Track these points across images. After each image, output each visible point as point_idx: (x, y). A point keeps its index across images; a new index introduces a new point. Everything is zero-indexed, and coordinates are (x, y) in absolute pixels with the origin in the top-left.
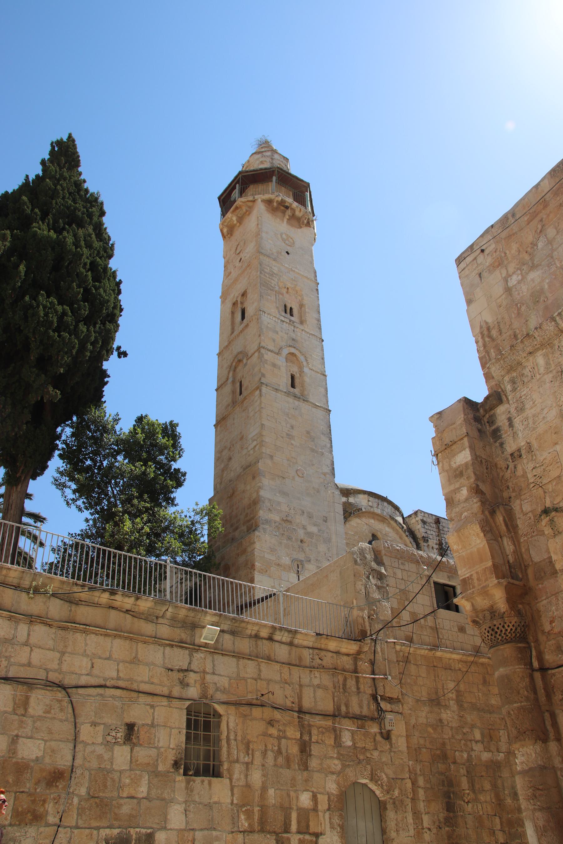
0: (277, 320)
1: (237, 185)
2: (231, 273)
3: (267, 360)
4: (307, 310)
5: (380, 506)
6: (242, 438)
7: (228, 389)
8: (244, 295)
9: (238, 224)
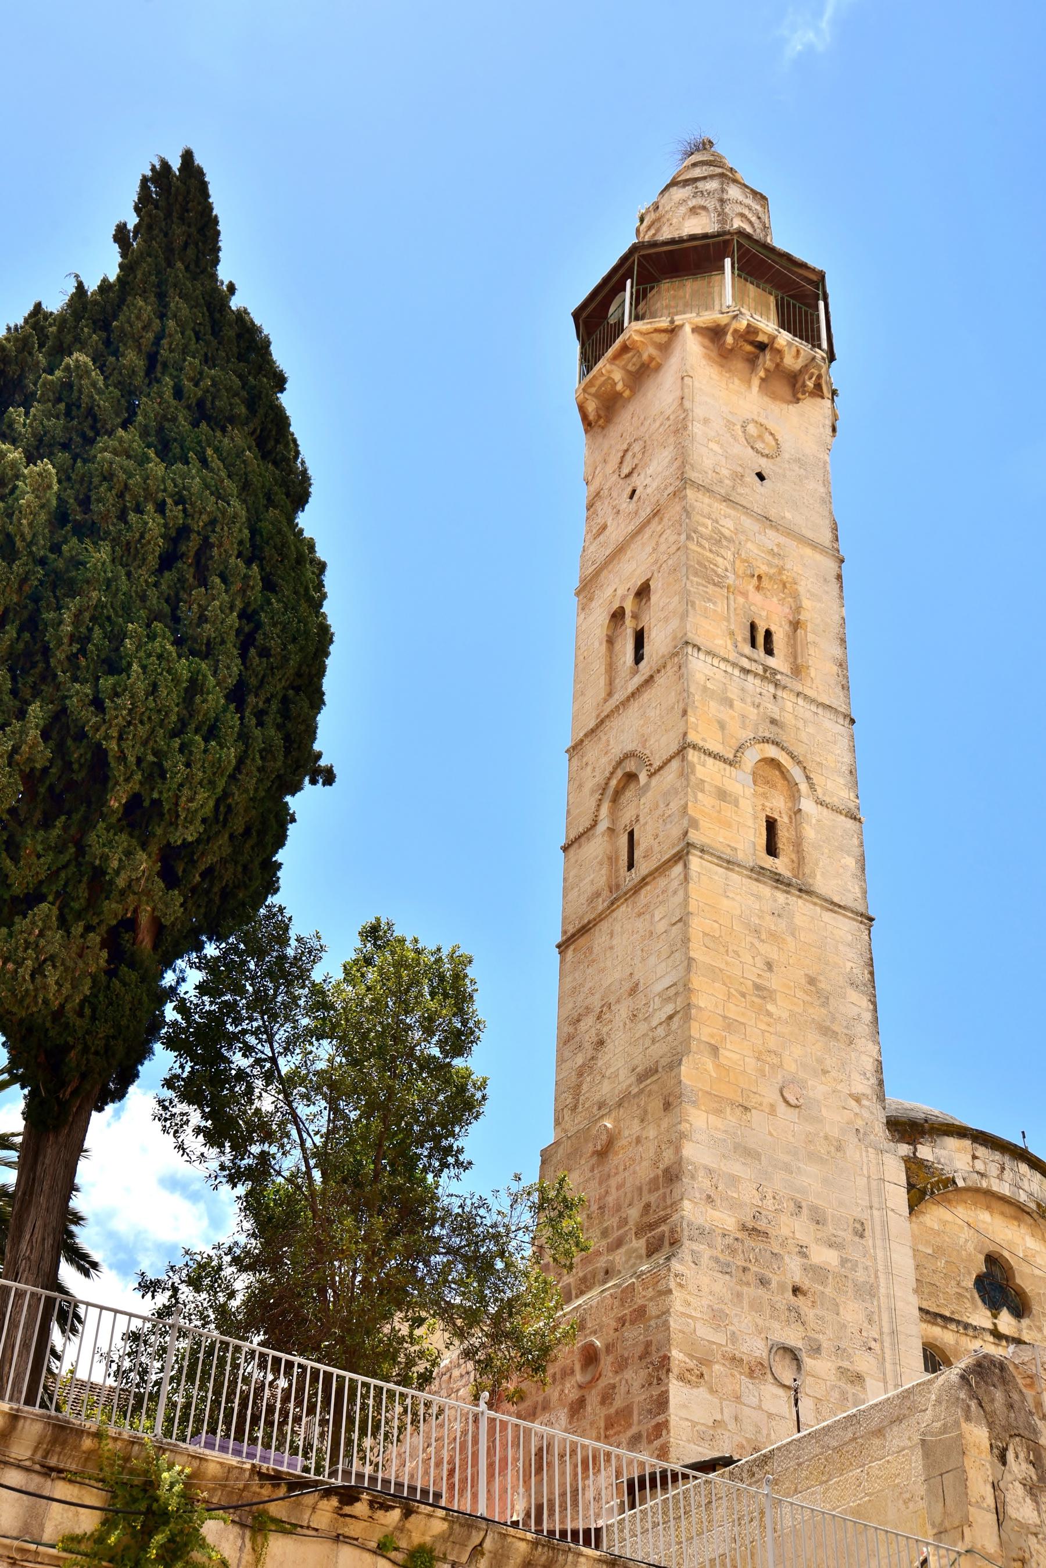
0: (730, 669)
1: (629, 282)
2: (604, 527)
3: (703, 781)
4: (811, 637)
5: (1008, 1175)
6: (633, 991)
8: (643, 592)
9: (627, 393)
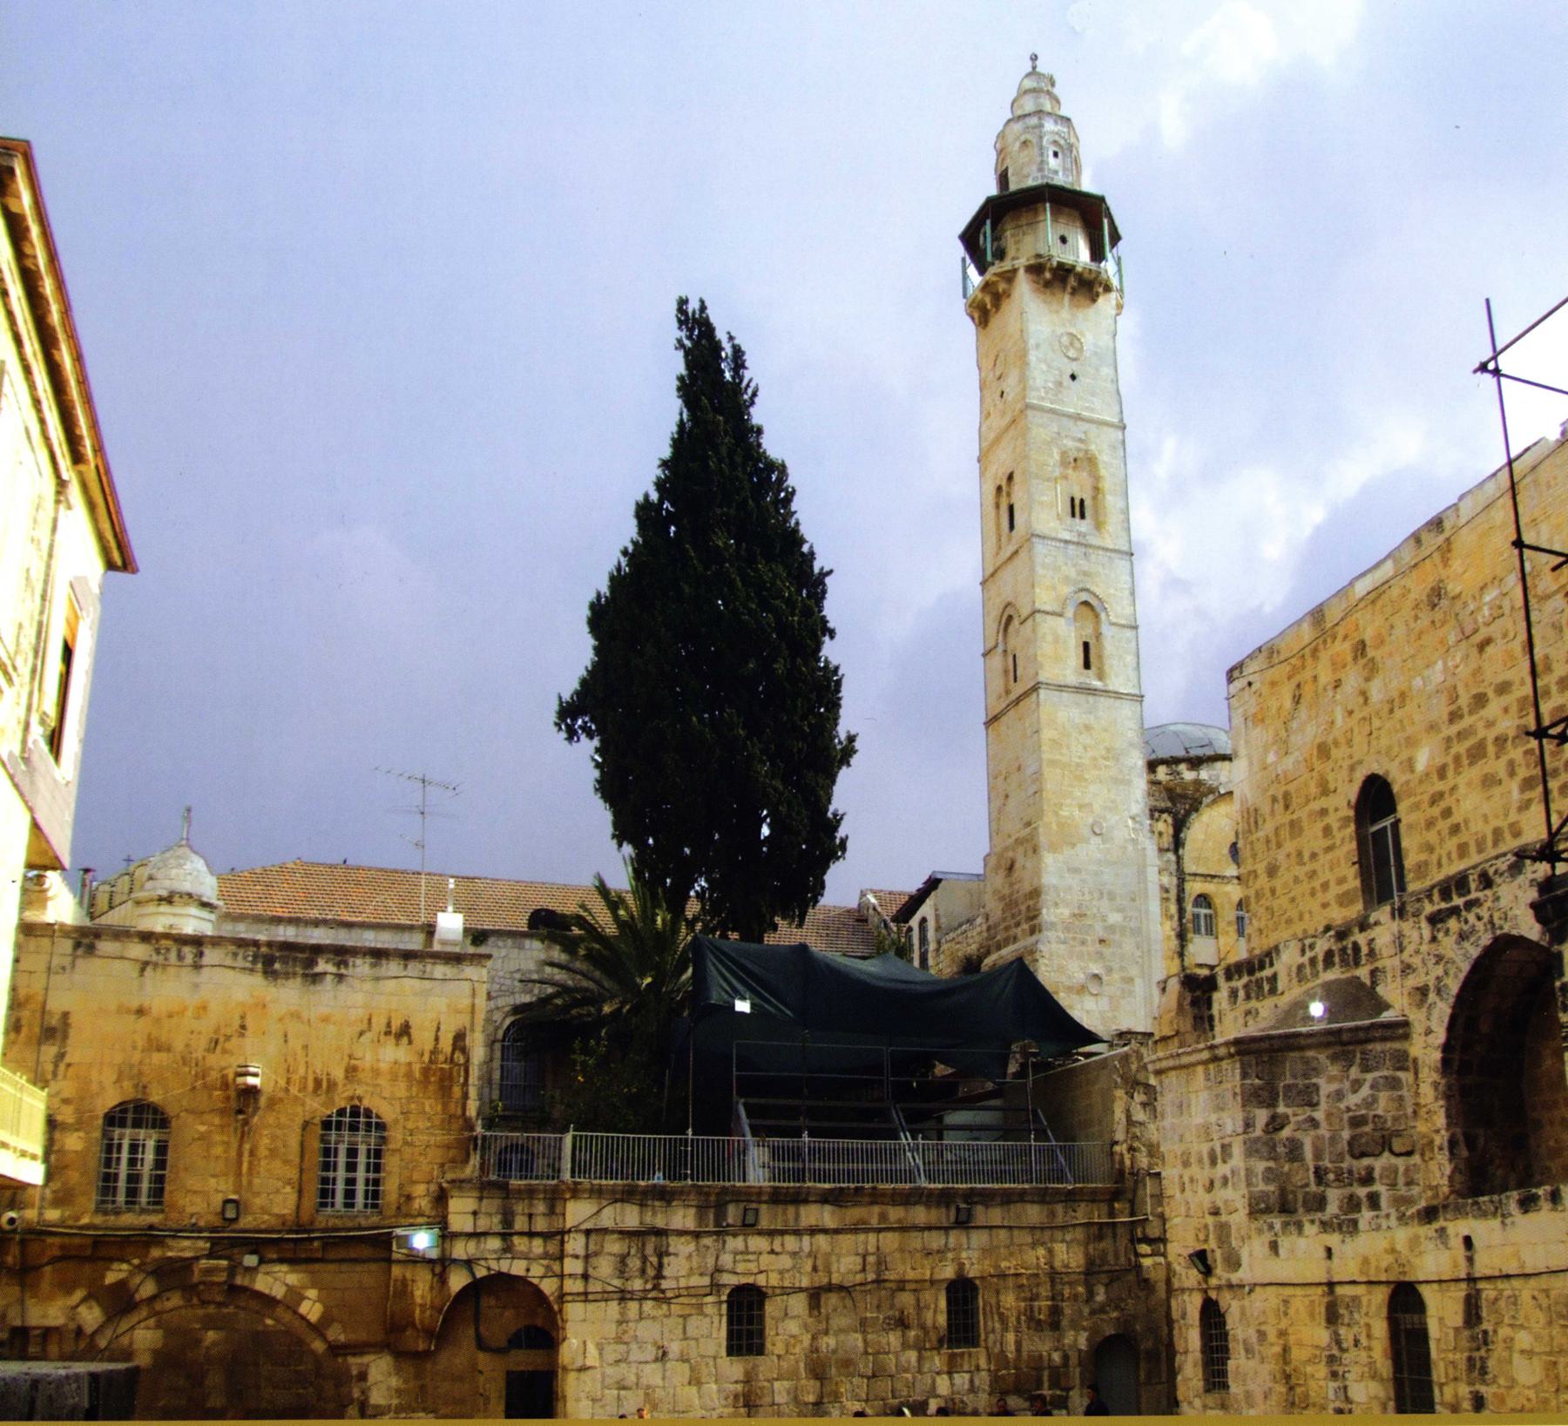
7: (997, 661)
